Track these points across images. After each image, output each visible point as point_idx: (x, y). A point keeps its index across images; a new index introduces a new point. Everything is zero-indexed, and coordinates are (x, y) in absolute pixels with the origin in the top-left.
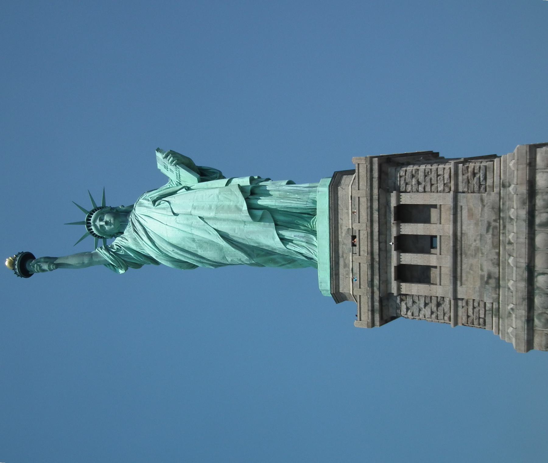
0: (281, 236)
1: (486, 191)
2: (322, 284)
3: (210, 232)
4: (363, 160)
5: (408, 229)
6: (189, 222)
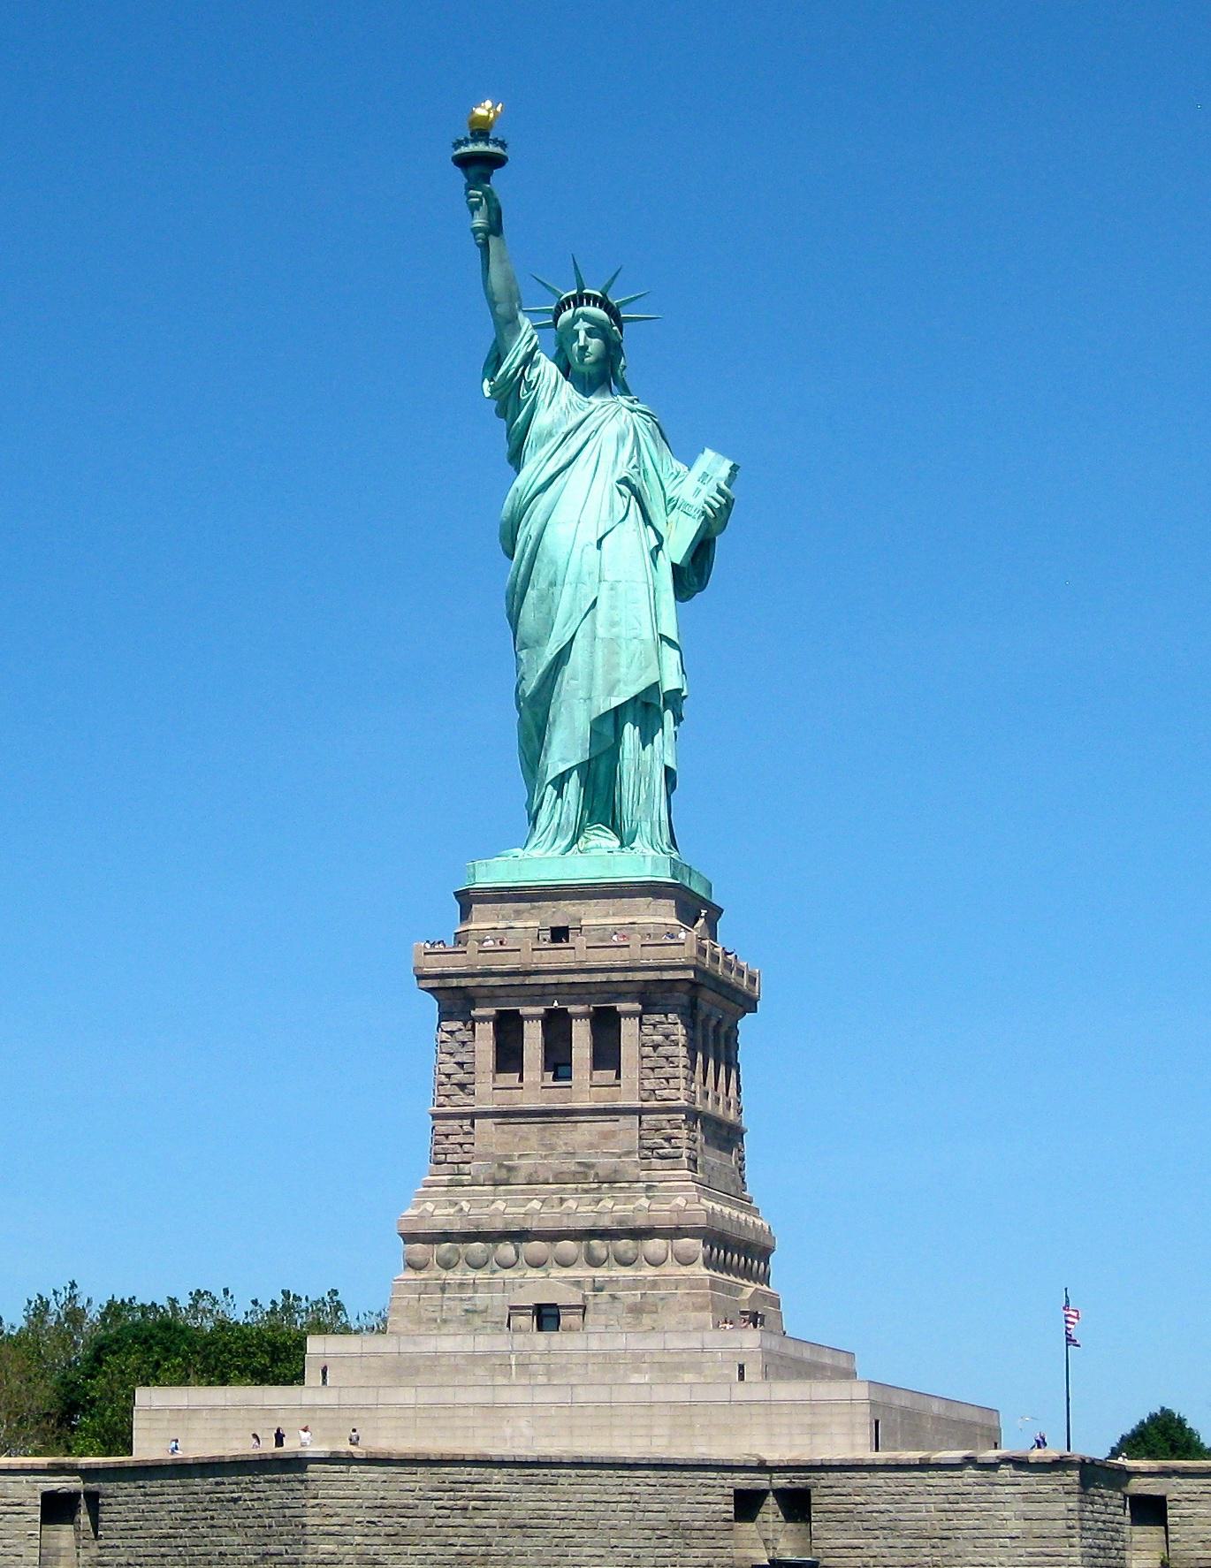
0: (567, 774)
1: (643, 1159)
2: (484, 868)
3: (568, 626)
5: (581, 1033)
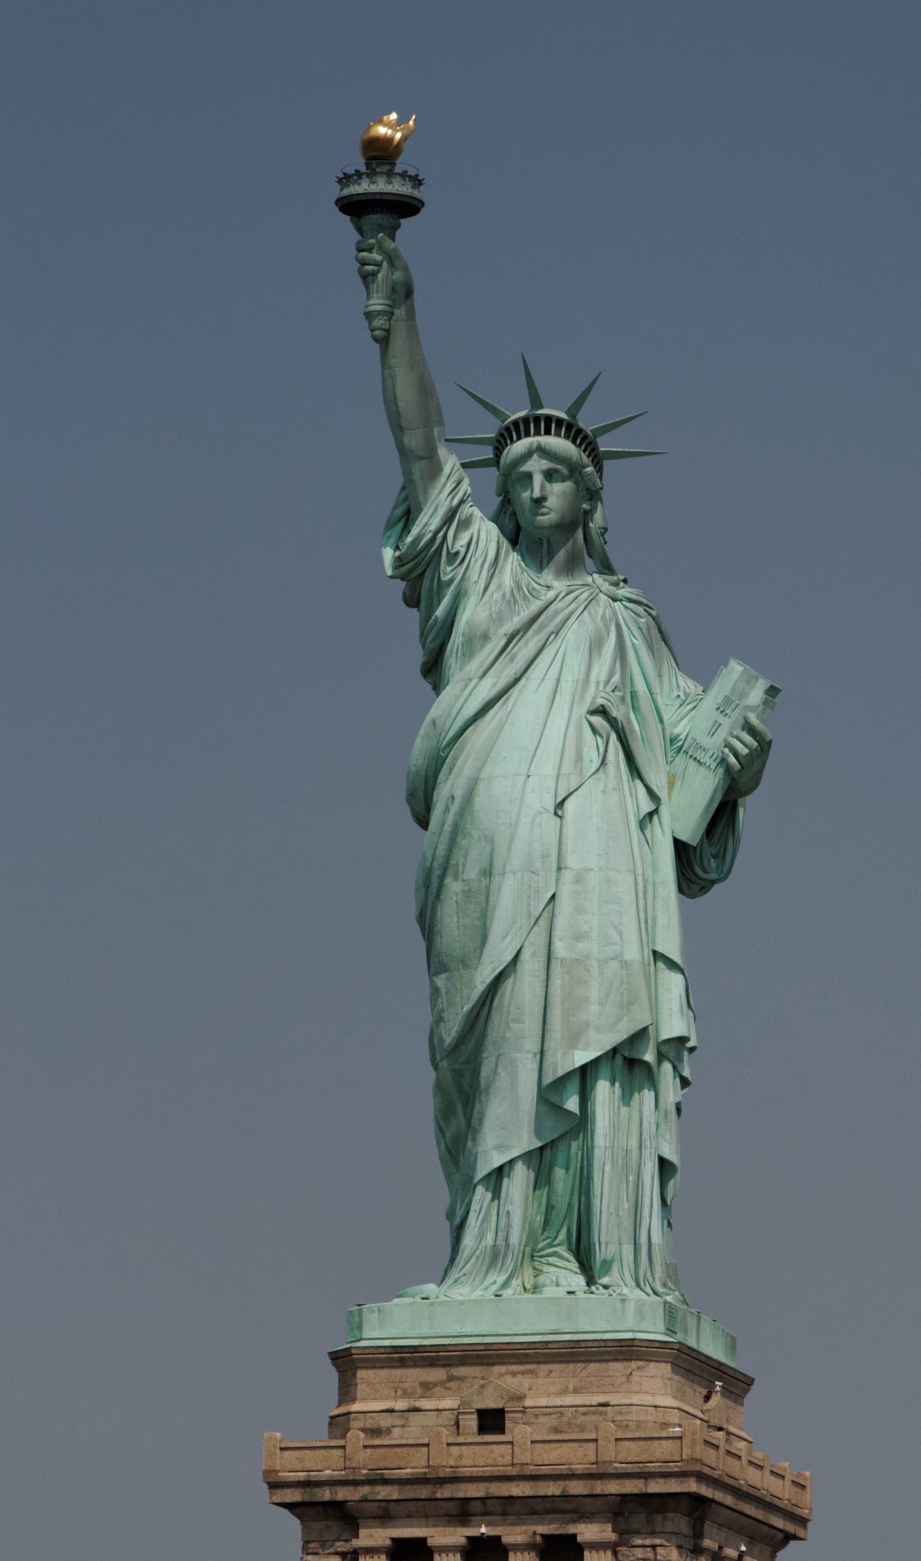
0: (506, 1169)
2: (376, 1315)
3: (509, 937)
4: (690, 1453)
6: (538, 865)
